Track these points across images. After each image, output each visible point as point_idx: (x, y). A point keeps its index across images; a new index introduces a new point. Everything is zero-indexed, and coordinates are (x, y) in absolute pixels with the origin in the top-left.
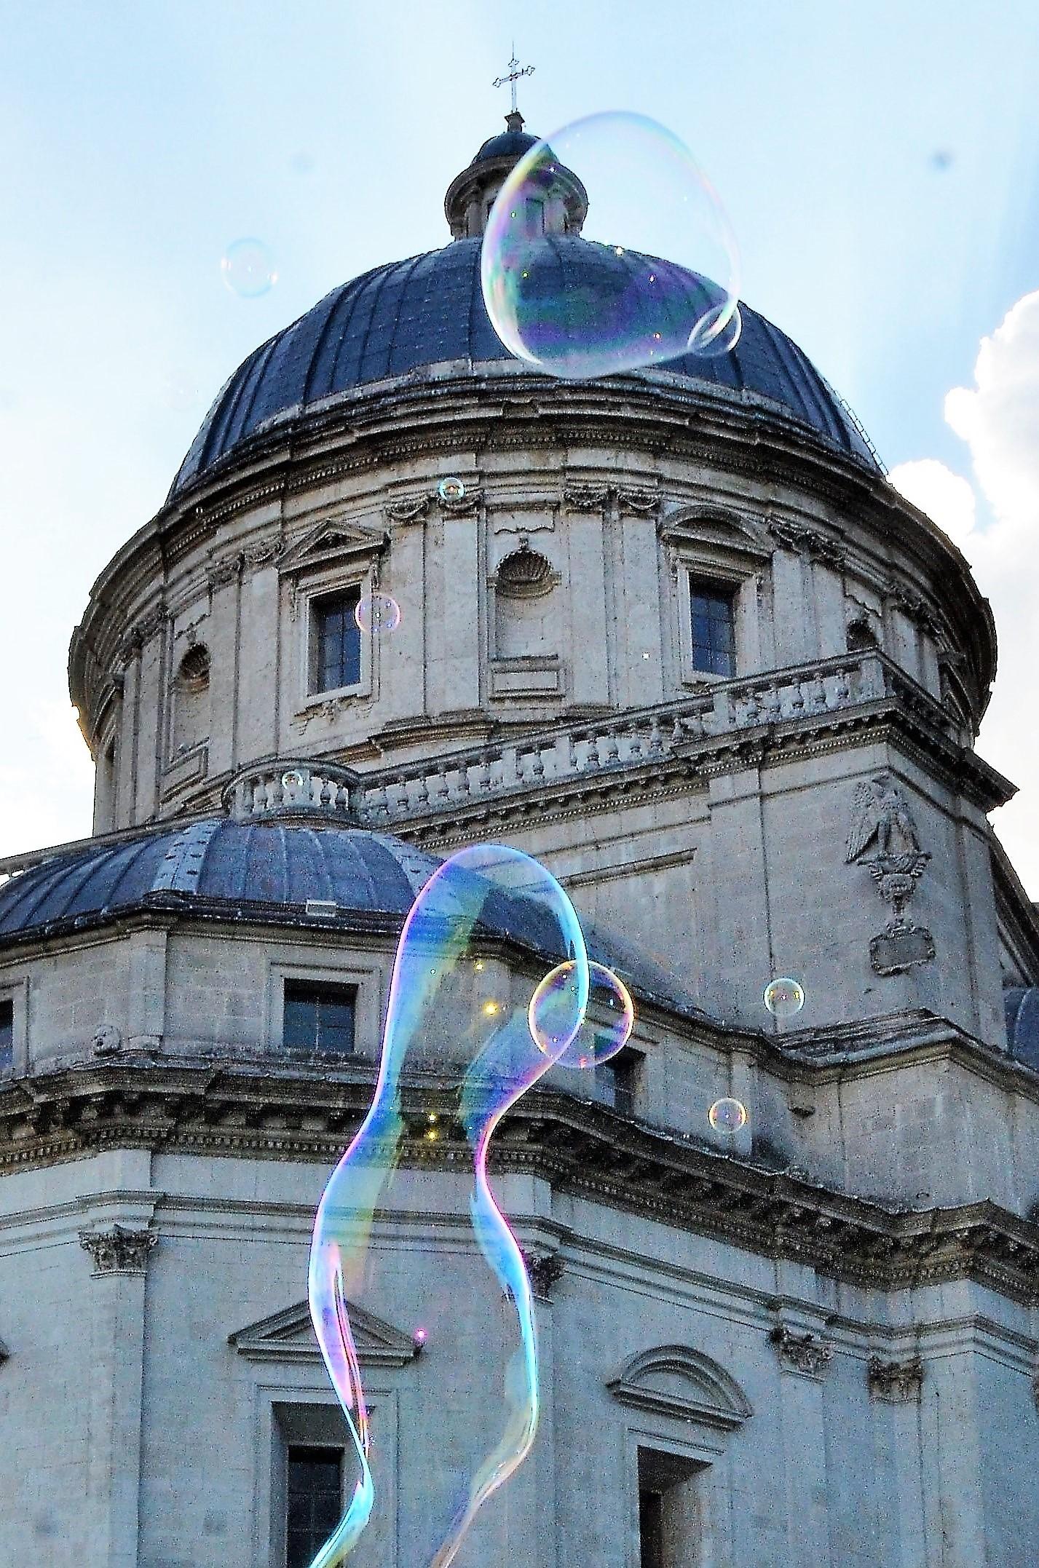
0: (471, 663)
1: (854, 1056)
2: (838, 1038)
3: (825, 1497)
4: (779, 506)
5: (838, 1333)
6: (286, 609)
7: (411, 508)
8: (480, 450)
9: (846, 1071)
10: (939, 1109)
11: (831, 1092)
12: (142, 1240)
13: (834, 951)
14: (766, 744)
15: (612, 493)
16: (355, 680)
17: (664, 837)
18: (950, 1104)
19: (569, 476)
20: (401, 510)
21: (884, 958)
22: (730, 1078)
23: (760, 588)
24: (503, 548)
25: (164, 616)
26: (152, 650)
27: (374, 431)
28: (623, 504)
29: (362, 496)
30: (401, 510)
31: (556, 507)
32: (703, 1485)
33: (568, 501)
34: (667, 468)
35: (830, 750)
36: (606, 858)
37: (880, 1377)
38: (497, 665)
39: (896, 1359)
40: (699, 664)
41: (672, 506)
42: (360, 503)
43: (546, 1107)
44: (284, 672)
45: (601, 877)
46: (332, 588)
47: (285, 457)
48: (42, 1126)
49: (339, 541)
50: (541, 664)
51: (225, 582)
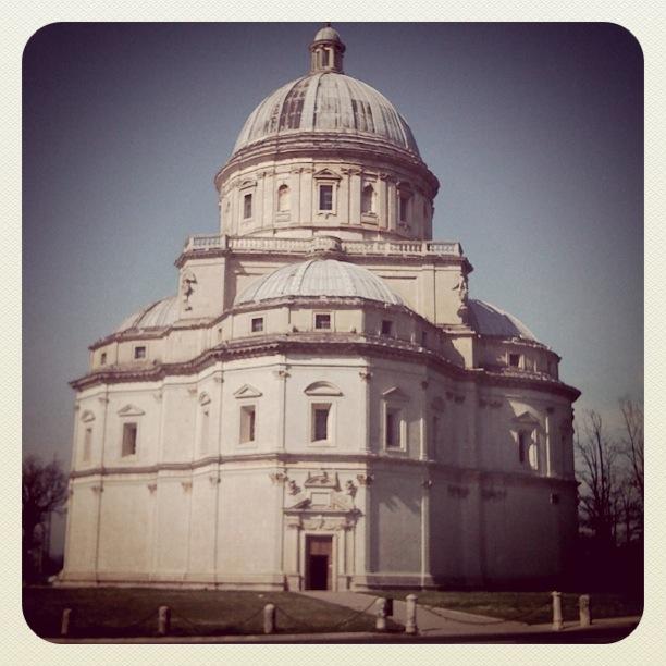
16: (330, 208)
24: (367, 184)
25: (275, 173)
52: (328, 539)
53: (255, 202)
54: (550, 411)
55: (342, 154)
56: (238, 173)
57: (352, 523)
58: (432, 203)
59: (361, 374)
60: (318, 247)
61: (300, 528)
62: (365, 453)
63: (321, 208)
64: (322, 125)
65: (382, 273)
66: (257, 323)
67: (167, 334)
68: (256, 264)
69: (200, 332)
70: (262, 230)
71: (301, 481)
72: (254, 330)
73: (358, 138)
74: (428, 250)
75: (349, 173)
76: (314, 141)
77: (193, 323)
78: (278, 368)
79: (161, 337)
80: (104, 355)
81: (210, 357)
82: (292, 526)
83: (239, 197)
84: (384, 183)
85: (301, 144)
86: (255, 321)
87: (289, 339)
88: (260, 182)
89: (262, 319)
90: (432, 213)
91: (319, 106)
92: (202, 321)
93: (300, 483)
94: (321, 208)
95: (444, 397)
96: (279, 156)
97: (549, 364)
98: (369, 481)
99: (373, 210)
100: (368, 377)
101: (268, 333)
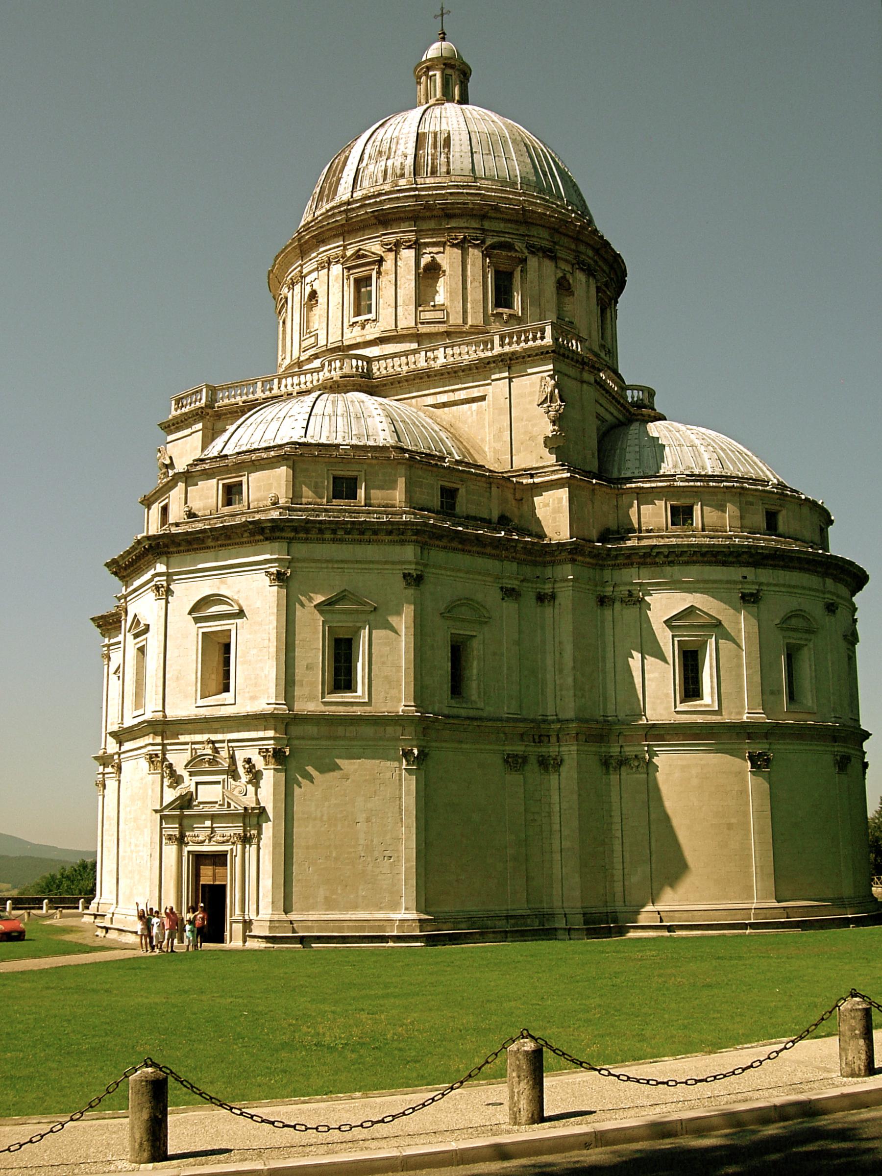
1: (537, 480)
3: (518, 643)
5: (525, 584)
6: (345, 281)
13: (532, 438)
16: (370, 312)
20: (387, 245)
22: (490, 493)
23: (522, 271)
24: (425, 260)
26: (297, 288)
32: (475, 644)
34: (487, 225)
37: (541, 598)
39: (546, 591)
40: (497, 304)
41: (489, 242)
47: (344, 222)
49: (364, 256)
51: (323, 268)
52: (219, 859)
54: (750, 599)
55: (383, 220)
57: (254, 832)
60: (328, 375)
61: (181, 841)
62: (269, 709)
63: (358, 313)
64: (366, 184)
65: (430, 400)
66: (165, 510)
71: (179, 759)
74: (502, 346)
75: (395, 248)
82: (170, 838)
84: (458, 252)
91: (366, 156)
93: (180, 770)
95: (491, 596)
98: (278, 756)
99: (440, 299)
100: (280, 578)
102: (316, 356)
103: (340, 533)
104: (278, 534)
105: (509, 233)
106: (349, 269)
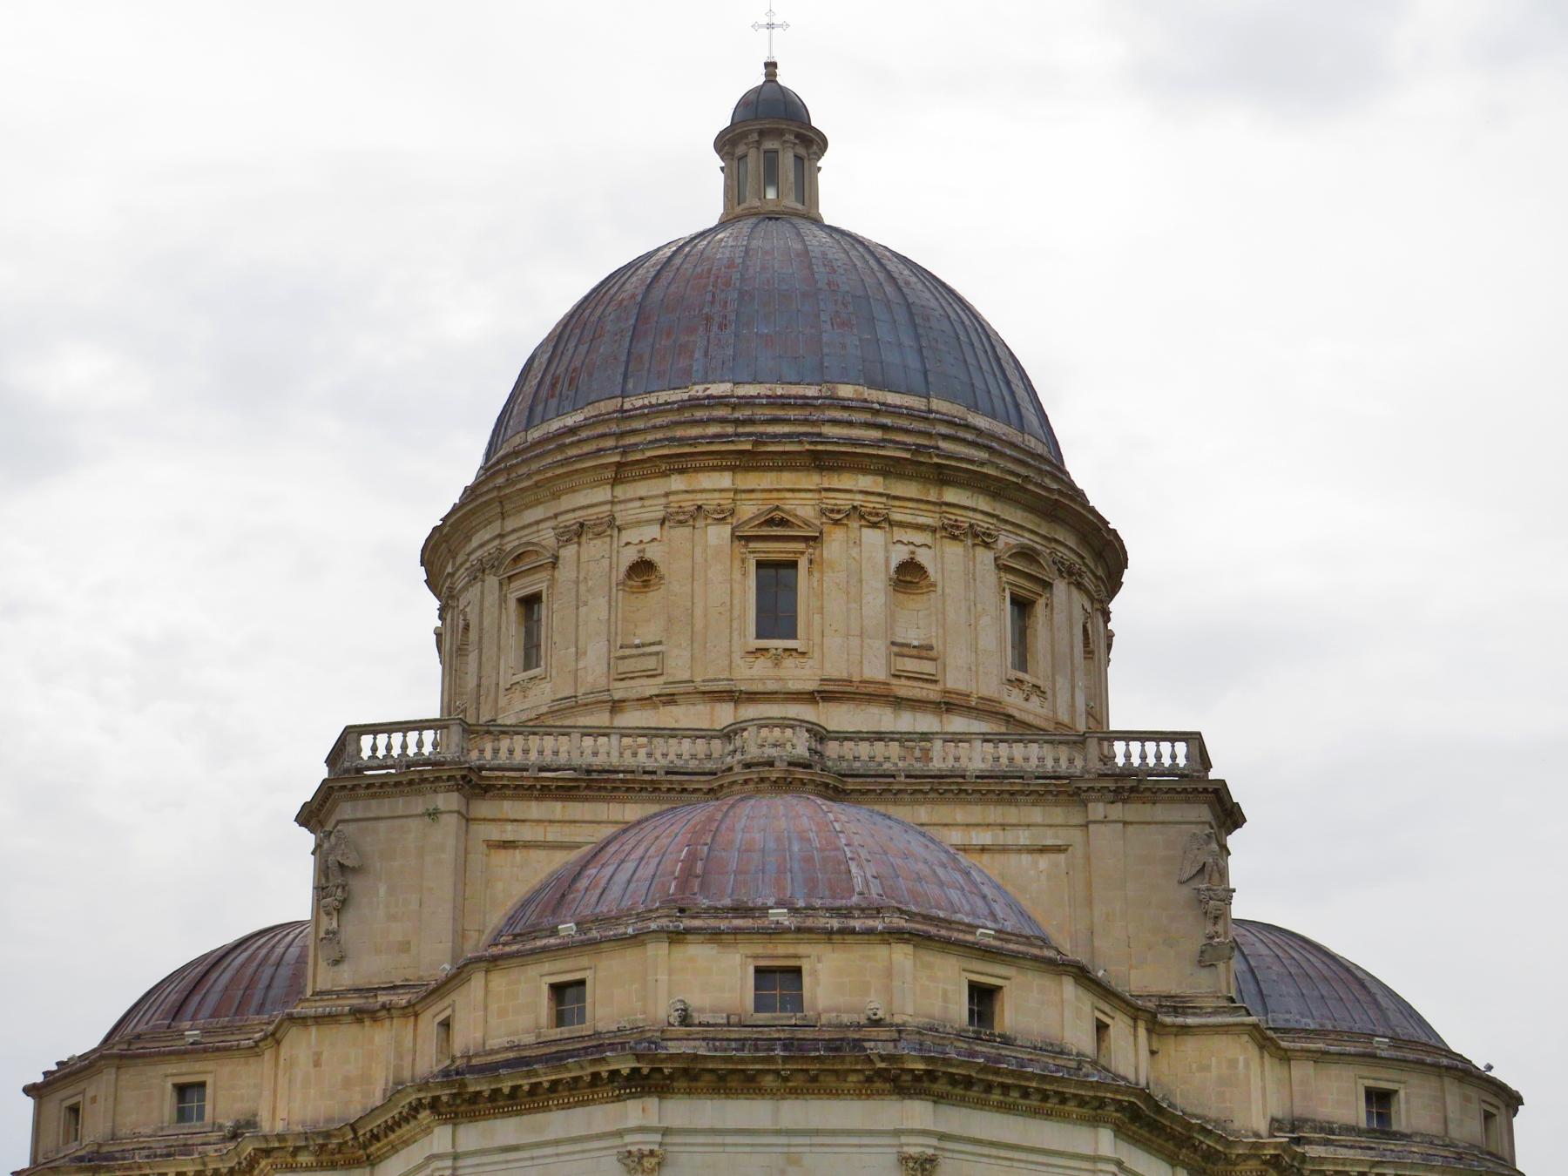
0: (878, 647)
1: (1190, 1021)
2: (1178, 1005)
4: (1056, 541)
7: (839, 512)
8: (885, 474)
9: (1185, 1030)
10: (1241, 1064)
11: (1171, 1040)
12: (932, 1160)
14: (1132, 790)
15: (971, 526)
16: (794, 636)
17: (1050, 832)
18: (1247, 1065)
19: (944, 508)
20: (832, 511)
21: (1207, 957)
24: (900, 555)
26: (594, 548)
27: (820, 448)
28: (976, 535)
29: (799, 490)
30: (832, 511)
31: (934, 531)
33: (944, 528)
35: (1172, 801)
36: (1009, 837)
38: (895, 649)
40: (1014, 667)
41: (1007, 540)
42: (797, 495)
43: (1131, 1095)
44: (736, 613)
45: (1004, 849)
46: (773, 557)
47: (749, 447)
48: (869, 1080)
49: (783, 523)
50: (924, 653)
53: (553, 616)
55: (821, 461)
56: (495, 528)
58: (1106, 616)
59: (904, 1160)
60: (753, 752)
65: (956, 837)
66: (566, 994)
67: (275, 1038)
68: (557, 809)
69: (381, 1036)
70: (572, 705)
72: (560, 1019)
73: (877, 412)
76: (737, 422)
77: (357, 1002)
78: (636, 1142)
79: (255, 1050)
80: (74, 1110)
81: (415, 1109)
83: (503, 600)
85: (695, 431)
86: (558, 990)
87: (674, 1048)
88: (568, 553)
89: (581, 983)
90: (1109, 646)
92: (383, 998)
94: (759, 636)
96: (621, 474)
97: (1488, 1117)
101: (602, 1027)
102: (670, 699)
103: (1015, 1094)
104: (926, 1085)
105: (1032, 532)
106: (748, 539)
